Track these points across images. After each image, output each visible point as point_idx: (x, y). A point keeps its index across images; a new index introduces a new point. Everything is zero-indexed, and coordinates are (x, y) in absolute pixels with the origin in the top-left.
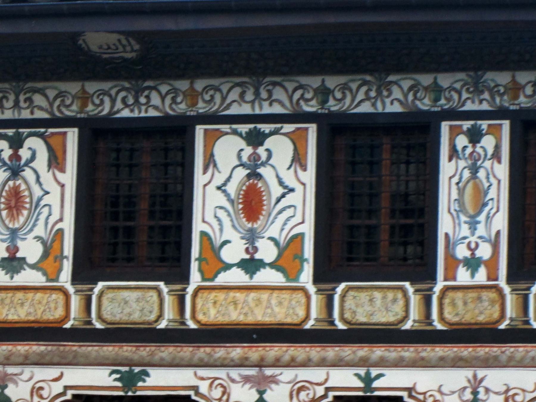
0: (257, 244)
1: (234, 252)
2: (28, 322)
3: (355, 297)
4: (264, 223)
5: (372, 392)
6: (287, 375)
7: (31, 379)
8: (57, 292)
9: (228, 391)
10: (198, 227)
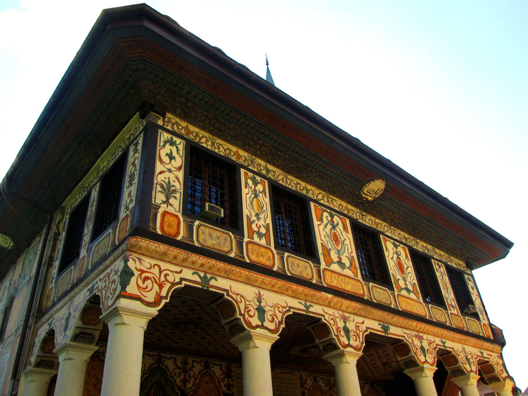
1: (402, 283)
2: (352, 292)
6: (425, 336)
7: (354, 321)
10: (391, 272)
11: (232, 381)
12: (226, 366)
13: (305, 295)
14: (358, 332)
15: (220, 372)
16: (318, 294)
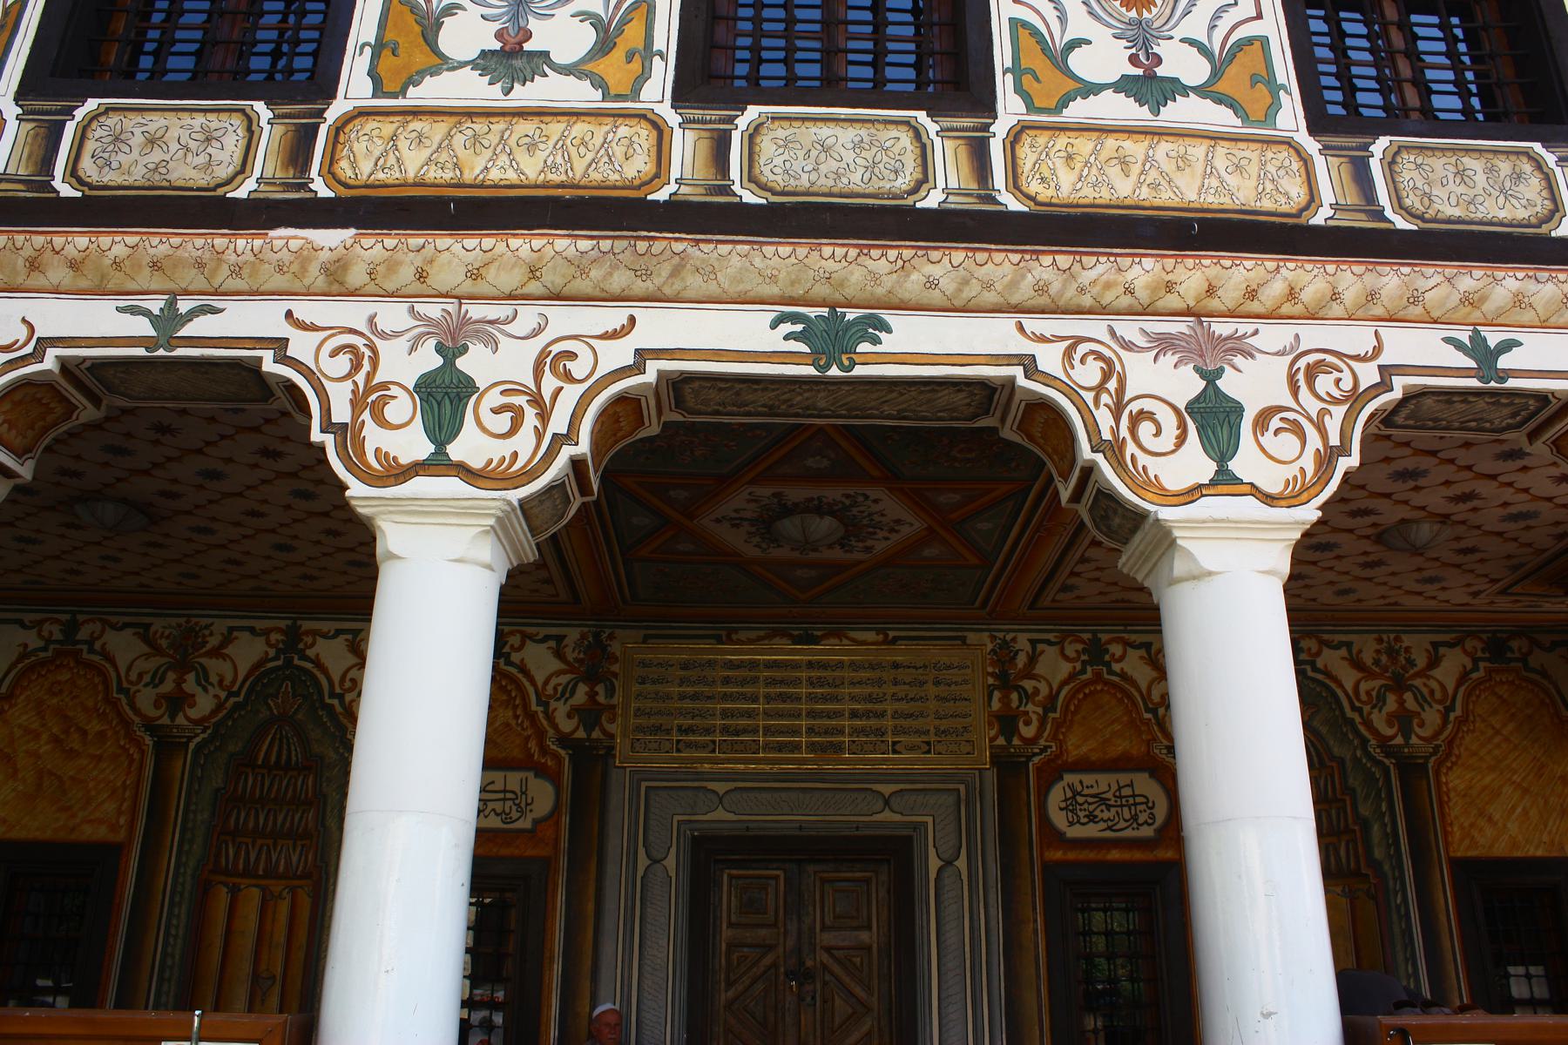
0: (1156, 50)
2: (546, 185)
3: (1418, 166)
4: (1168, 11)
5: (1503, 380)
6: (1273, 336)
7: (536, 333)
8: (634, 121)
9: (1118, 368)
11: (611, 692)
12: (583, 636)
13: (156, 265)
14: (549, 383)
15: (556, 665)
16: (243, 244)
